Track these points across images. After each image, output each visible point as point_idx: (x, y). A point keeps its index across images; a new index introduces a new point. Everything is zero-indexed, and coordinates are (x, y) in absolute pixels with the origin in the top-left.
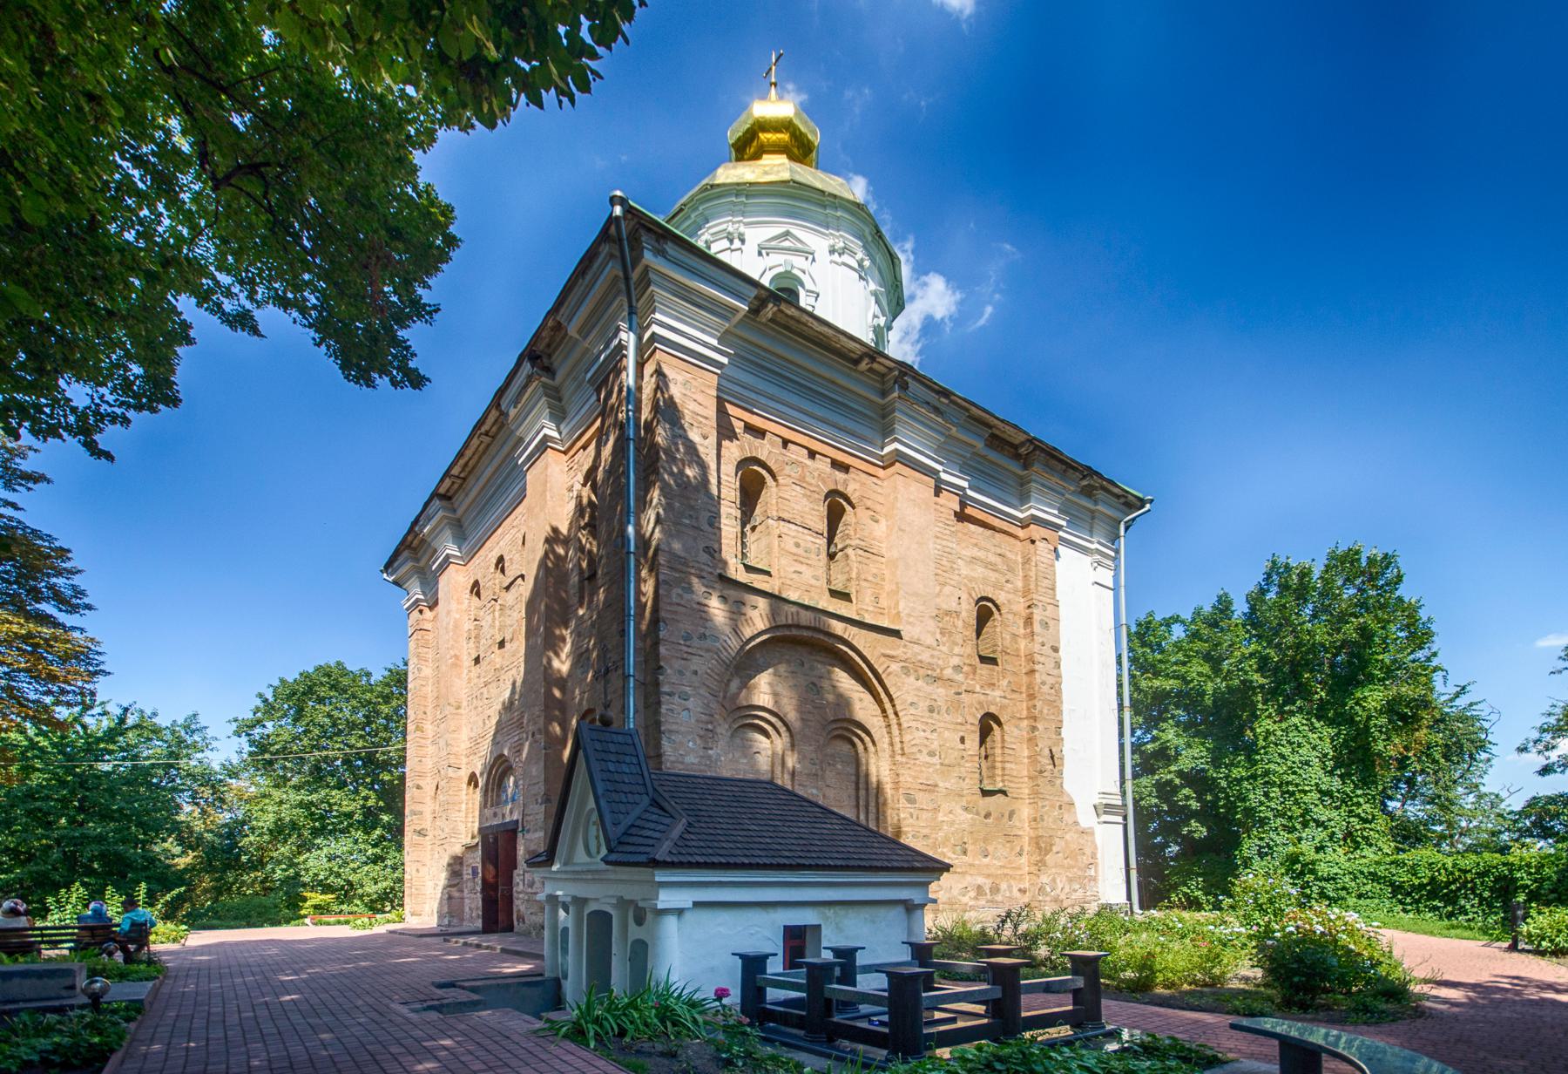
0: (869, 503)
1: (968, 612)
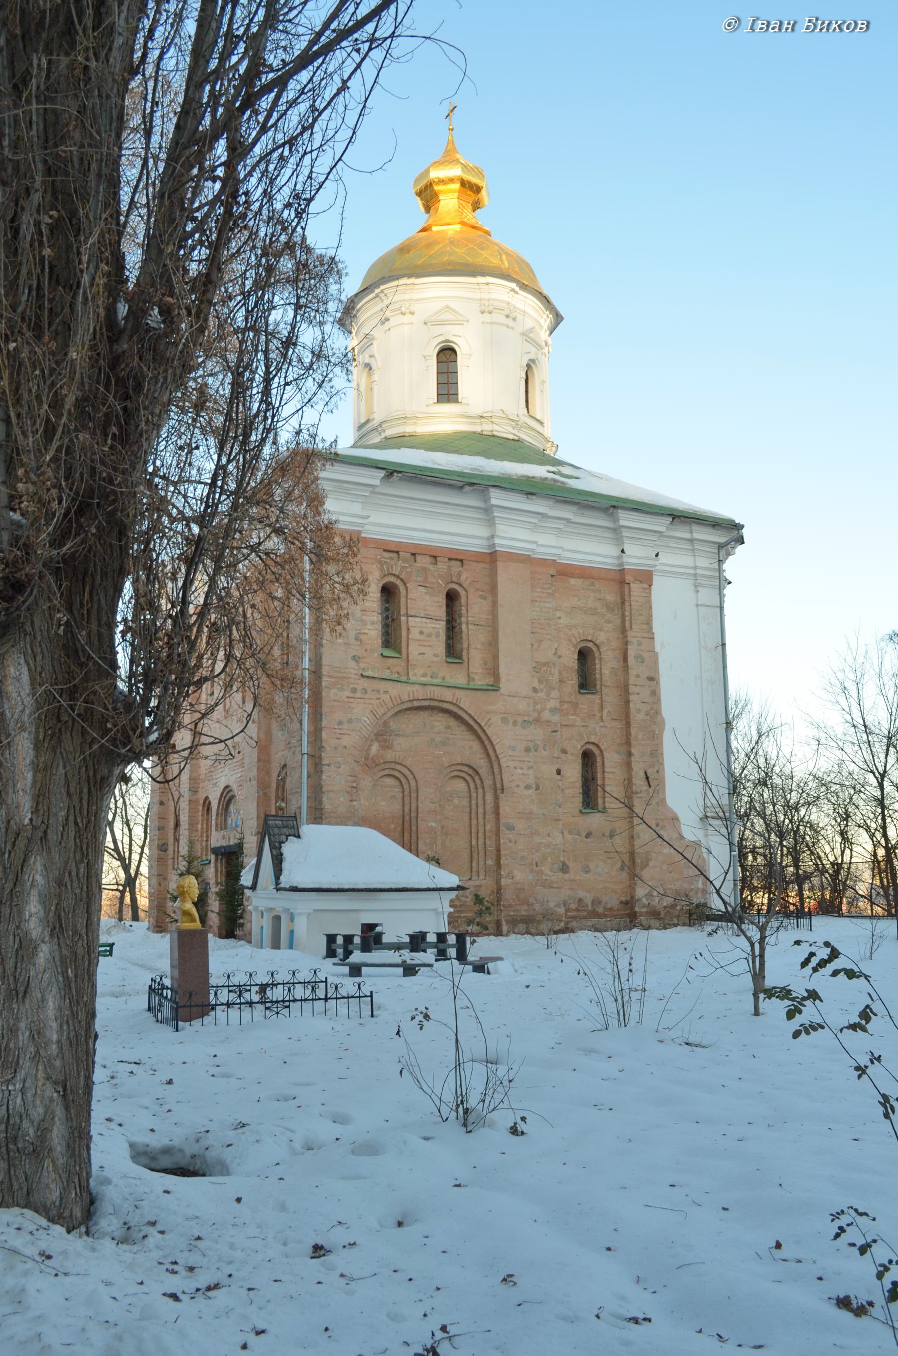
1: (571, 659)
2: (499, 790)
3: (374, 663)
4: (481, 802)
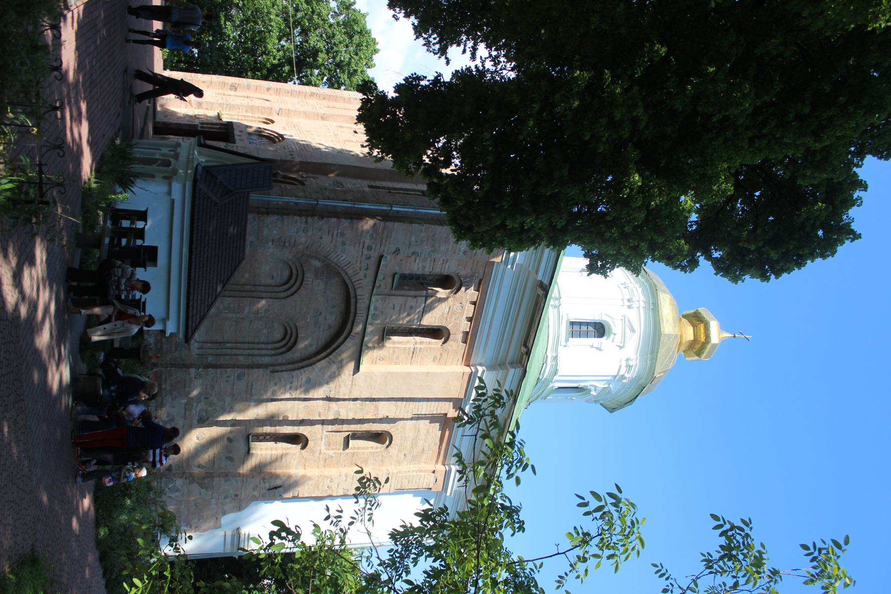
0: (445, 355)
3: (389, 265)
4: (264, 352)
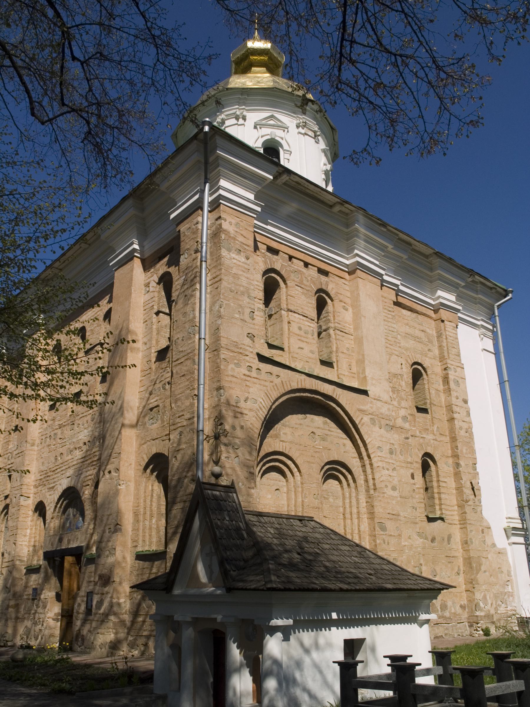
0: (341, 297)
2: (372, 489)
